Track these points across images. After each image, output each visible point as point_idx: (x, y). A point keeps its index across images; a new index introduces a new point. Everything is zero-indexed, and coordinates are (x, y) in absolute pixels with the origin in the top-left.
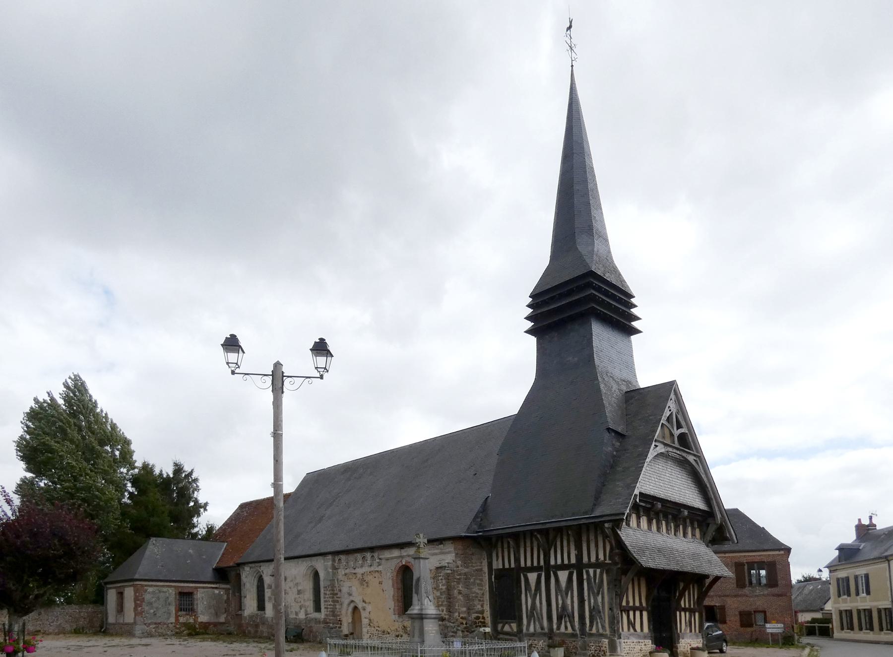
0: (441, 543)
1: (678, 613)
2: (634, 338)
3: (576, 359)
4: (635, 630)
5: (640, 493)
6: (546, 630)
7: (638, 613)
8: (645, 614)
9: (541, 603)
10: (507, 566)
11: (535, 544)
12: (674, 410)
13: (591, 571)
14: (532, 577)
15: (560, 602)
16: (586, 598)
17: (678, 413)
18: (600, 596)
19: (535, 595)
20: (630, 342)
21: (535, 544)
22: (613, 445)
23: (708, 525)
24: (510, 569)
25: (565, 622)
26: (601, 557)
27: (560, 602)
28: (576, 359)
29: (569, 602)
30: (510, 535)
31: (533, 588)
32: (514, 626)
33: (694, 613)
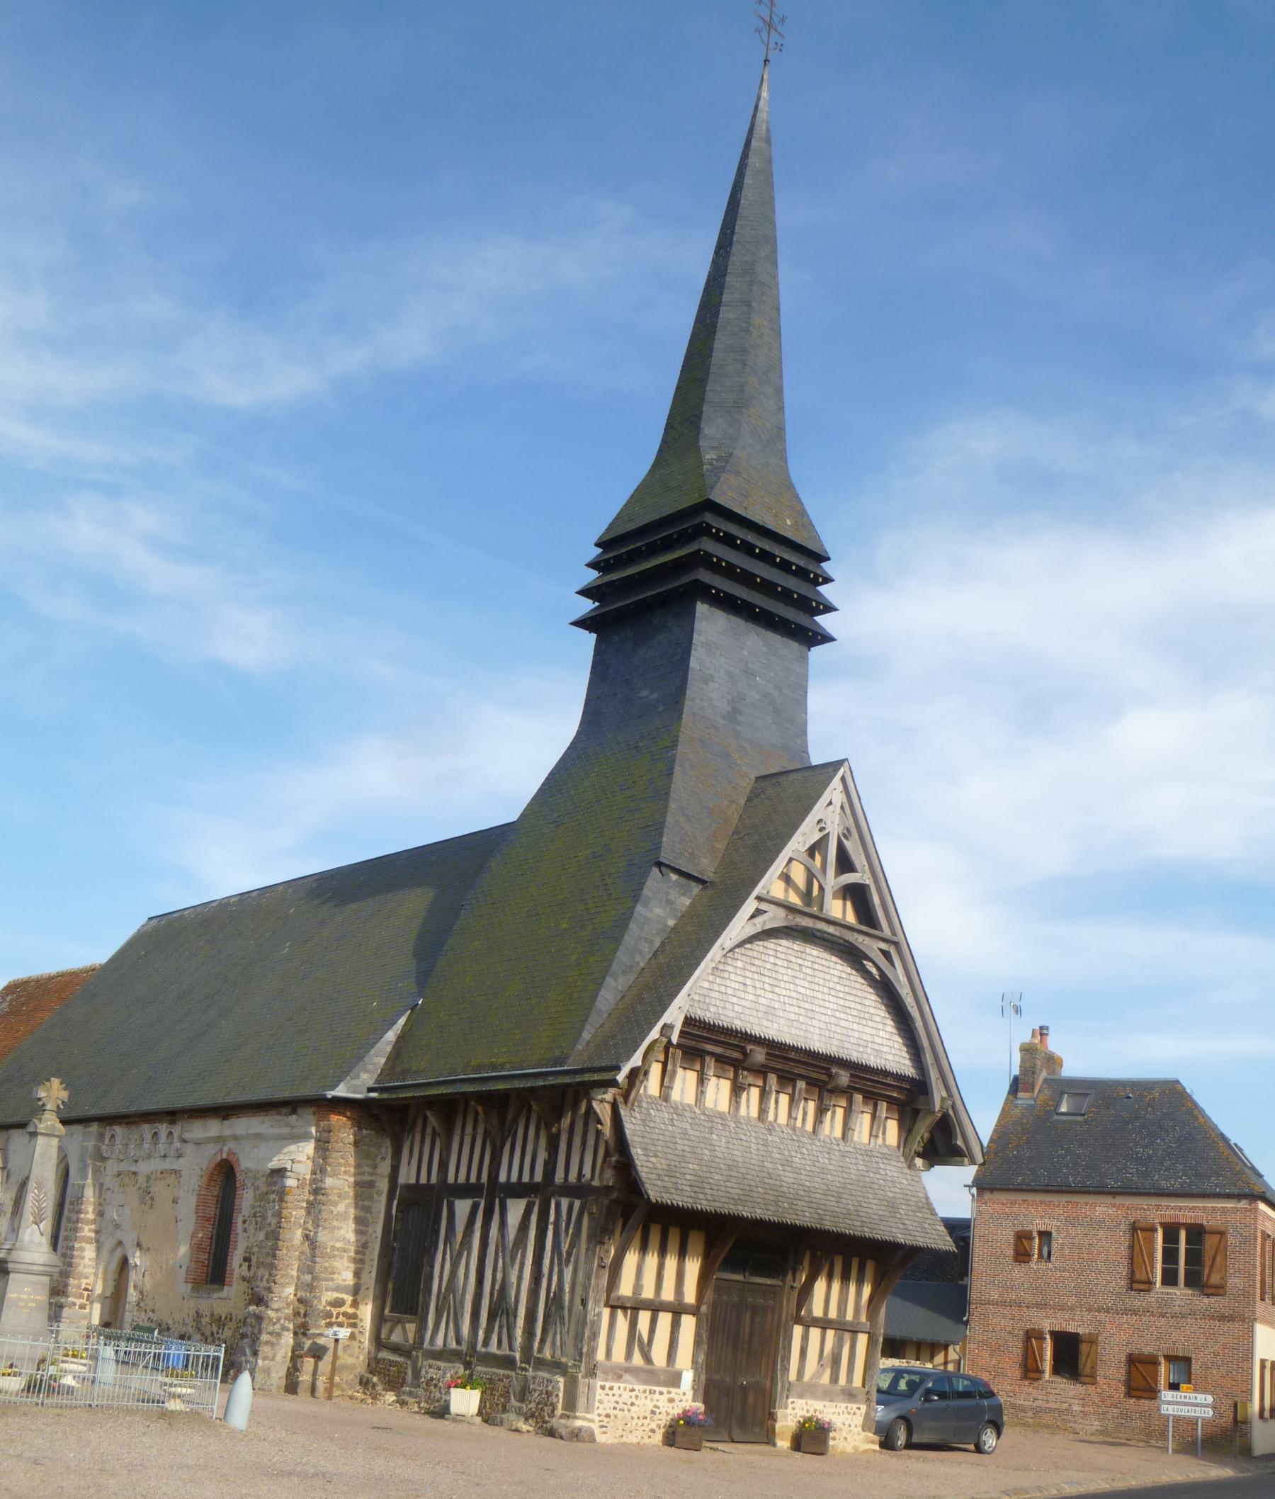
0: (294, 1112)
1: (798, 1330)
2: (817, 653)
3: (655, 696)
4: (647, 1358)
5: (689, 1021)
6: (464, 1347)
7: (665, 1319)
8: (688, 1324)
9: (520, 1278)
10: (423, 1180)
11: (480, 1130)
12: (834, 830)
13: (565, 1203)
14: (463, 1207)
15: (499, 1276)
16: (546, 1270)
17: (847, 834)
18: (571, 1267)
19: (460, 1254)
20: (805, 660)
21: (480, 1130)
22: (670, 902)
23: (916, 1113)
24: (429, 1186)
25: (500, 1327)
26: (587, 1171)
27: (499, 1276)
28: (655, 696)
29: (513, 1279)
30: (430, 1102)
31: (459, 1237)
32: (411, 1328)
33: (855, 1332)
